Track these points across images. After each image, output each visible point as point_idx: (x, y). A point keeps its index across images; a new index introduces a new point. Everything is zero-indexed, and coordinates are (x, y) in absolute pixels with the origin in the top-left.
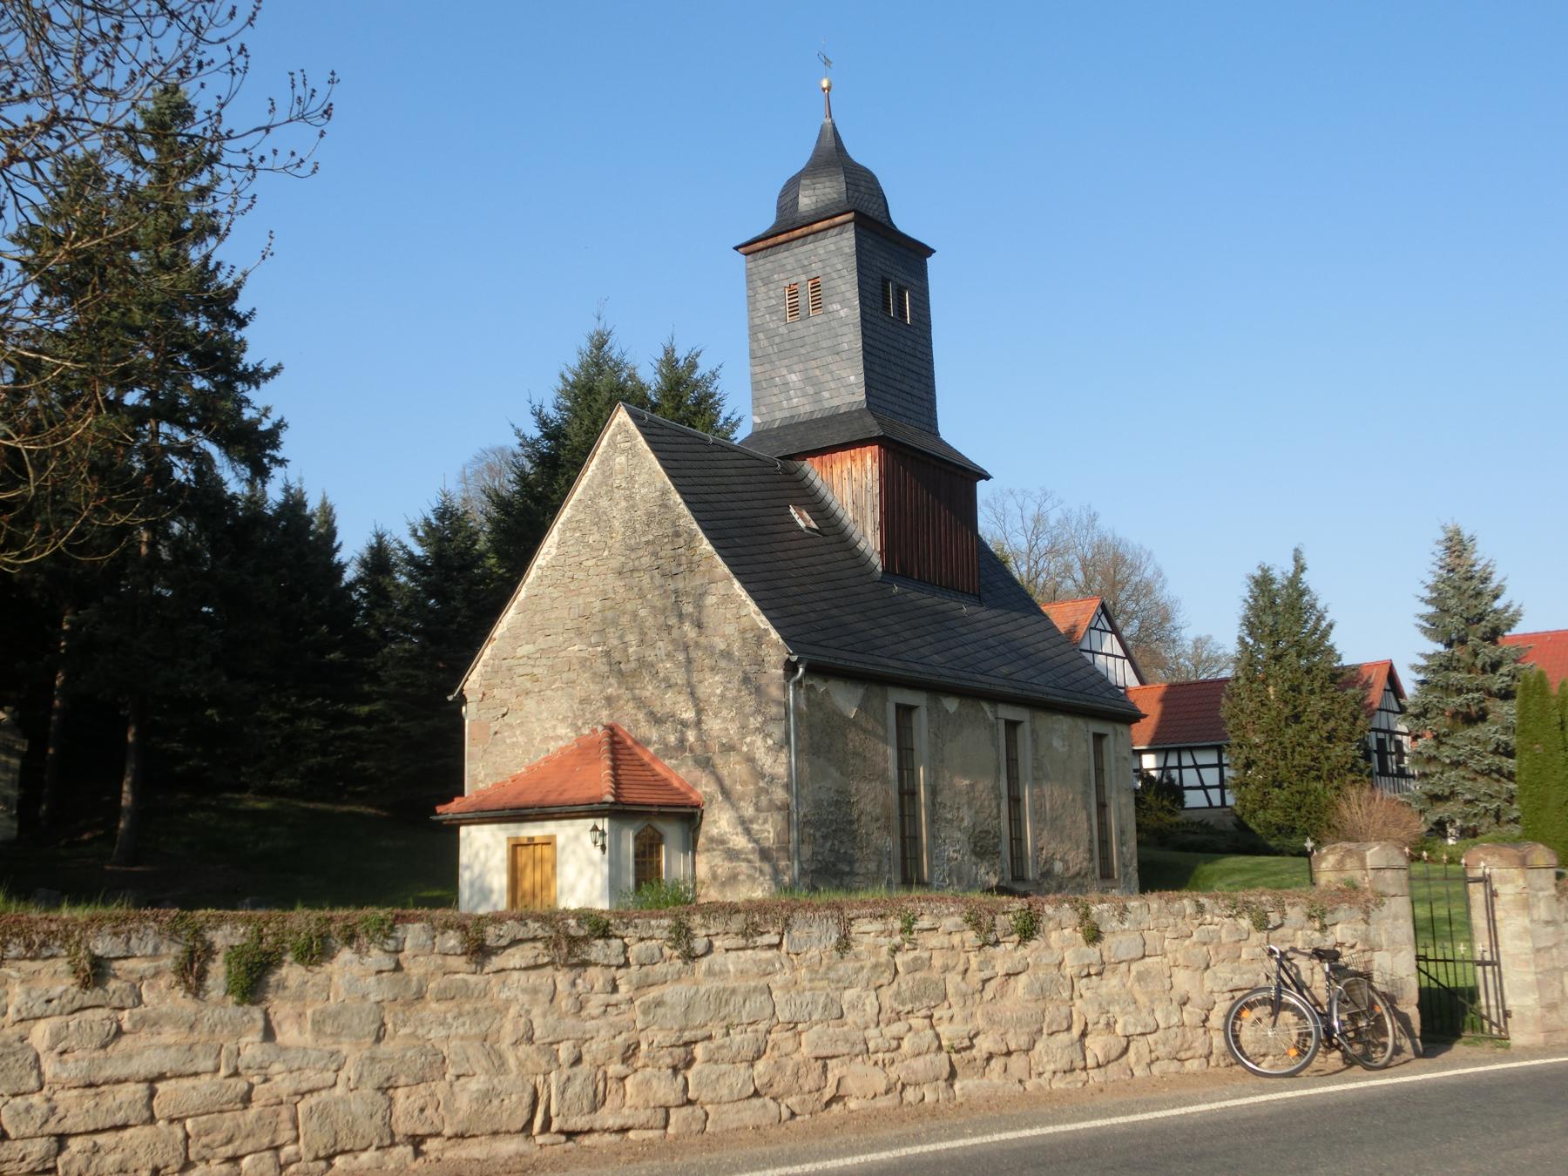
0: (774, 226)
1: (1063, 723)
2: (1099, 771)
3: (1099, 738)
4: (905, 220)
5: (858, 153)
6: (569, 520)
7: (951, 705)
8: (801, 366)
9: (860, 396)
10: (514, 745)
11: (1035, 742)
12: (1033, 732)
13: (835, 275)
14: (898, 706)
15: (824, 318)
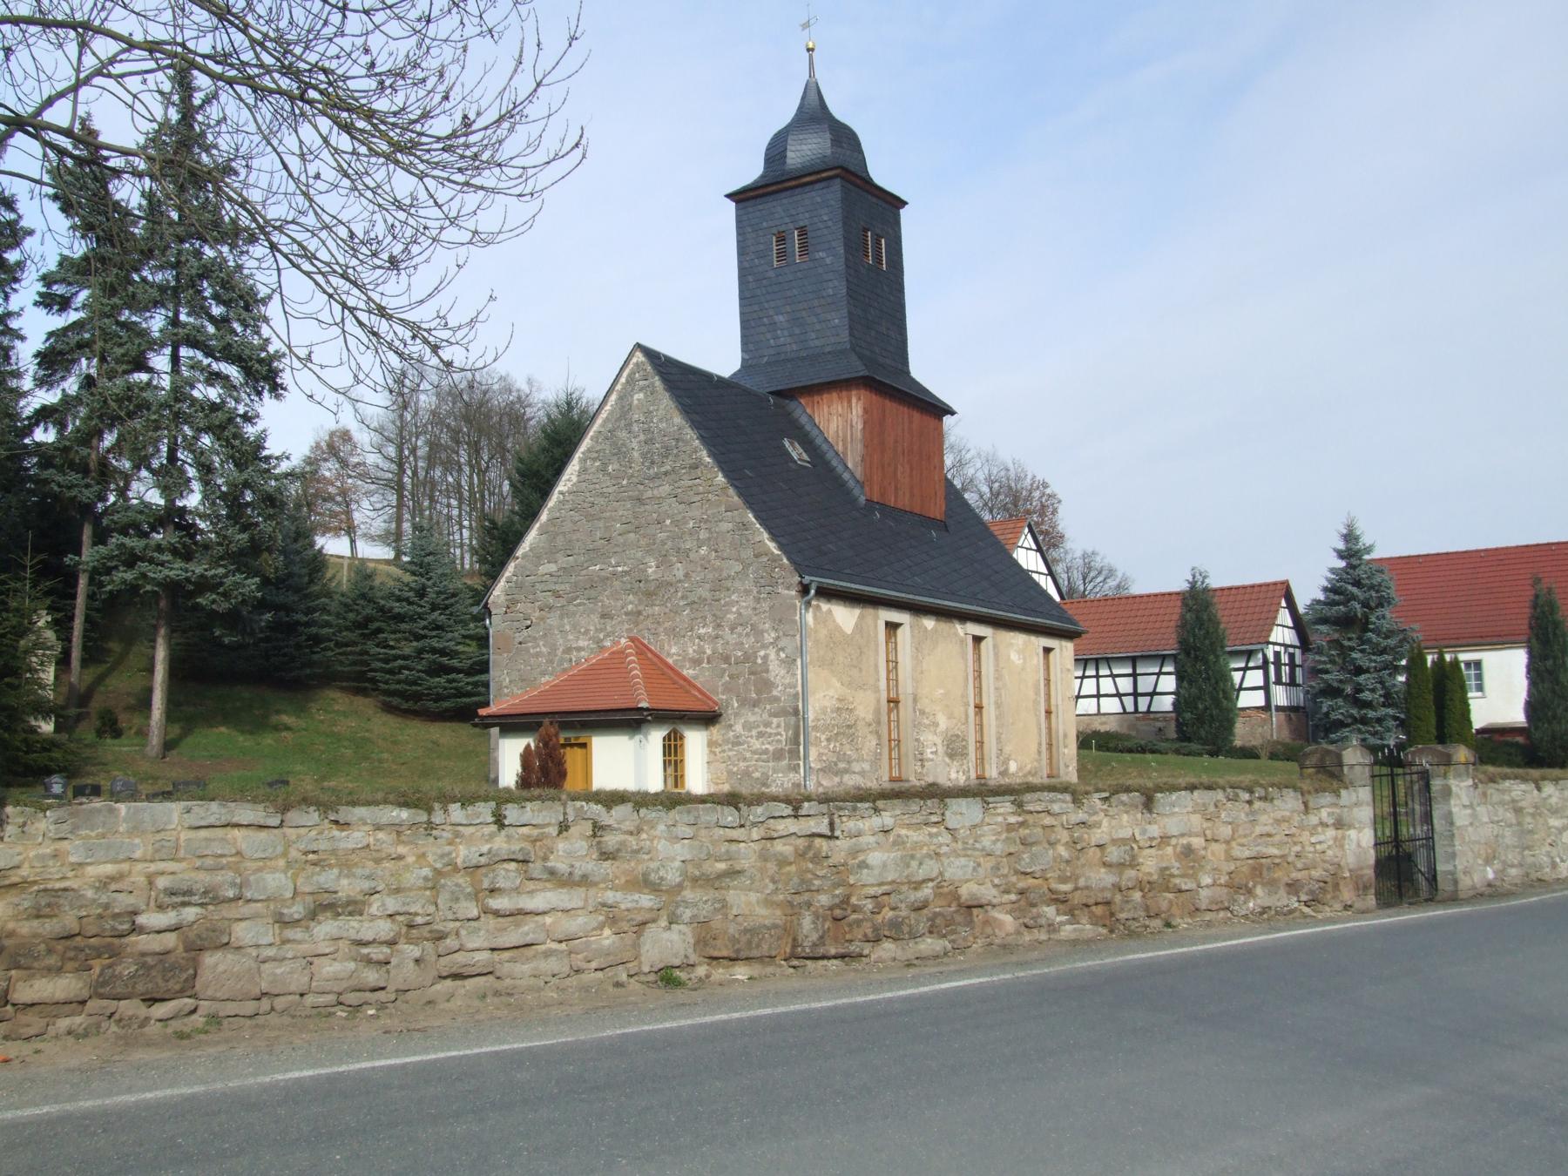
0: (762, 177)
1: (1019, 639)
2: (1048, 681)
3: (1047, 651)
4: (882, 173)
5: (839, 111)
6: (589, 450)
7: (929, 623)
8: (788, 309)
9: (844, 335)
10: (538, 655)
11: (996, 655)
12: (995, 646)
13: (821, 225)
14: (887, 624)
15: (811, 264)
